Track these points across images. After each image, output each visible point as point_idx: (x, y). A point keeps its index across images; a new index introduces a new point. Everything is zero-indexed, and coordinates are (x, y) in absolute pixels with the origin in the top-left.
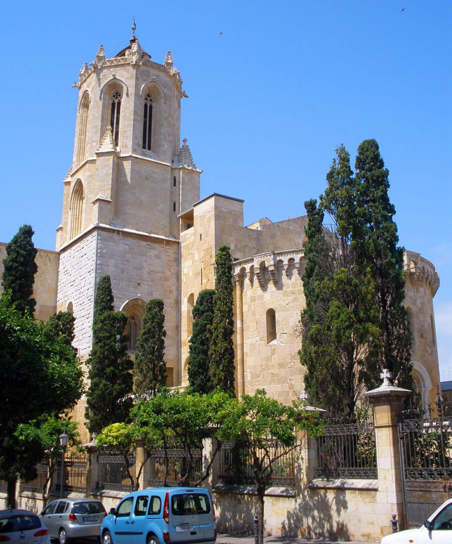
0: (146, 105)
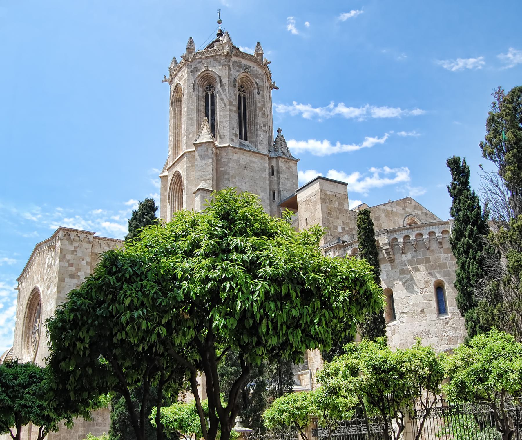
0: (239, 97)
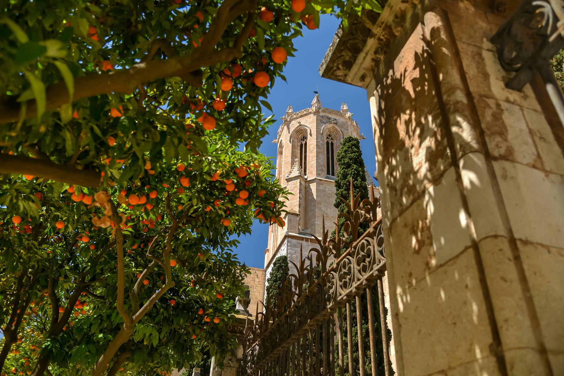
0: (328, 143)
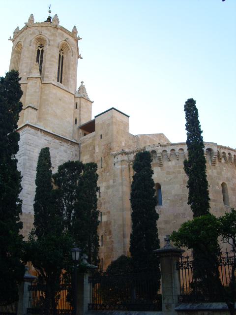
0: (60, 56)
